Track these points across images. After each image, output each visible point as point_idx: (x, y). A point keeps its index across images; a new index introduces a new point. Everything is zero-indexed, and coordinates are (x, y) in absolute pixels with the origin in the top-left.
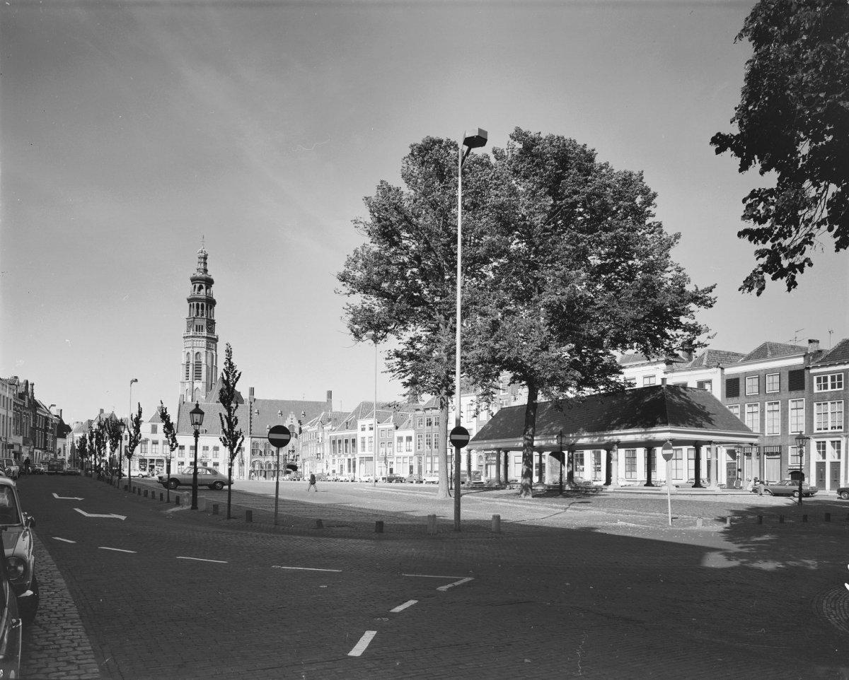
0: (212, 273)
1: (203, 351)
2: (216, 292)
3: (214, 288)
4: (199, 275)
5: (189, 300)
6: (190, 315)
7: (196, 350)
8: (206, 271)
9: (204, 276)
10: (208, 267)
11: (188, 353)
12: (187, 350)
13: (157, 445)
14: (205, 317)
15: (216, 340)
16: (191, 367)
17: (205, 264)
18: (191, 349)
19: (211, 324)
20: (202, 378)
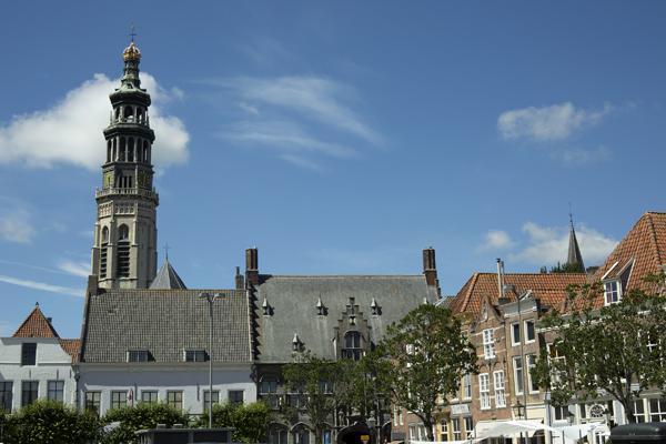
1: (132, 223)
4: (125, 89)
5: (108, 134)
6: (109, 160)
7: (120, 222)
8: (137, 83)
11: (106, 228)
12: (107, 222)
13: (27, 378)
18: (110, 219)
19: (147, 171)
20: (130, 272)
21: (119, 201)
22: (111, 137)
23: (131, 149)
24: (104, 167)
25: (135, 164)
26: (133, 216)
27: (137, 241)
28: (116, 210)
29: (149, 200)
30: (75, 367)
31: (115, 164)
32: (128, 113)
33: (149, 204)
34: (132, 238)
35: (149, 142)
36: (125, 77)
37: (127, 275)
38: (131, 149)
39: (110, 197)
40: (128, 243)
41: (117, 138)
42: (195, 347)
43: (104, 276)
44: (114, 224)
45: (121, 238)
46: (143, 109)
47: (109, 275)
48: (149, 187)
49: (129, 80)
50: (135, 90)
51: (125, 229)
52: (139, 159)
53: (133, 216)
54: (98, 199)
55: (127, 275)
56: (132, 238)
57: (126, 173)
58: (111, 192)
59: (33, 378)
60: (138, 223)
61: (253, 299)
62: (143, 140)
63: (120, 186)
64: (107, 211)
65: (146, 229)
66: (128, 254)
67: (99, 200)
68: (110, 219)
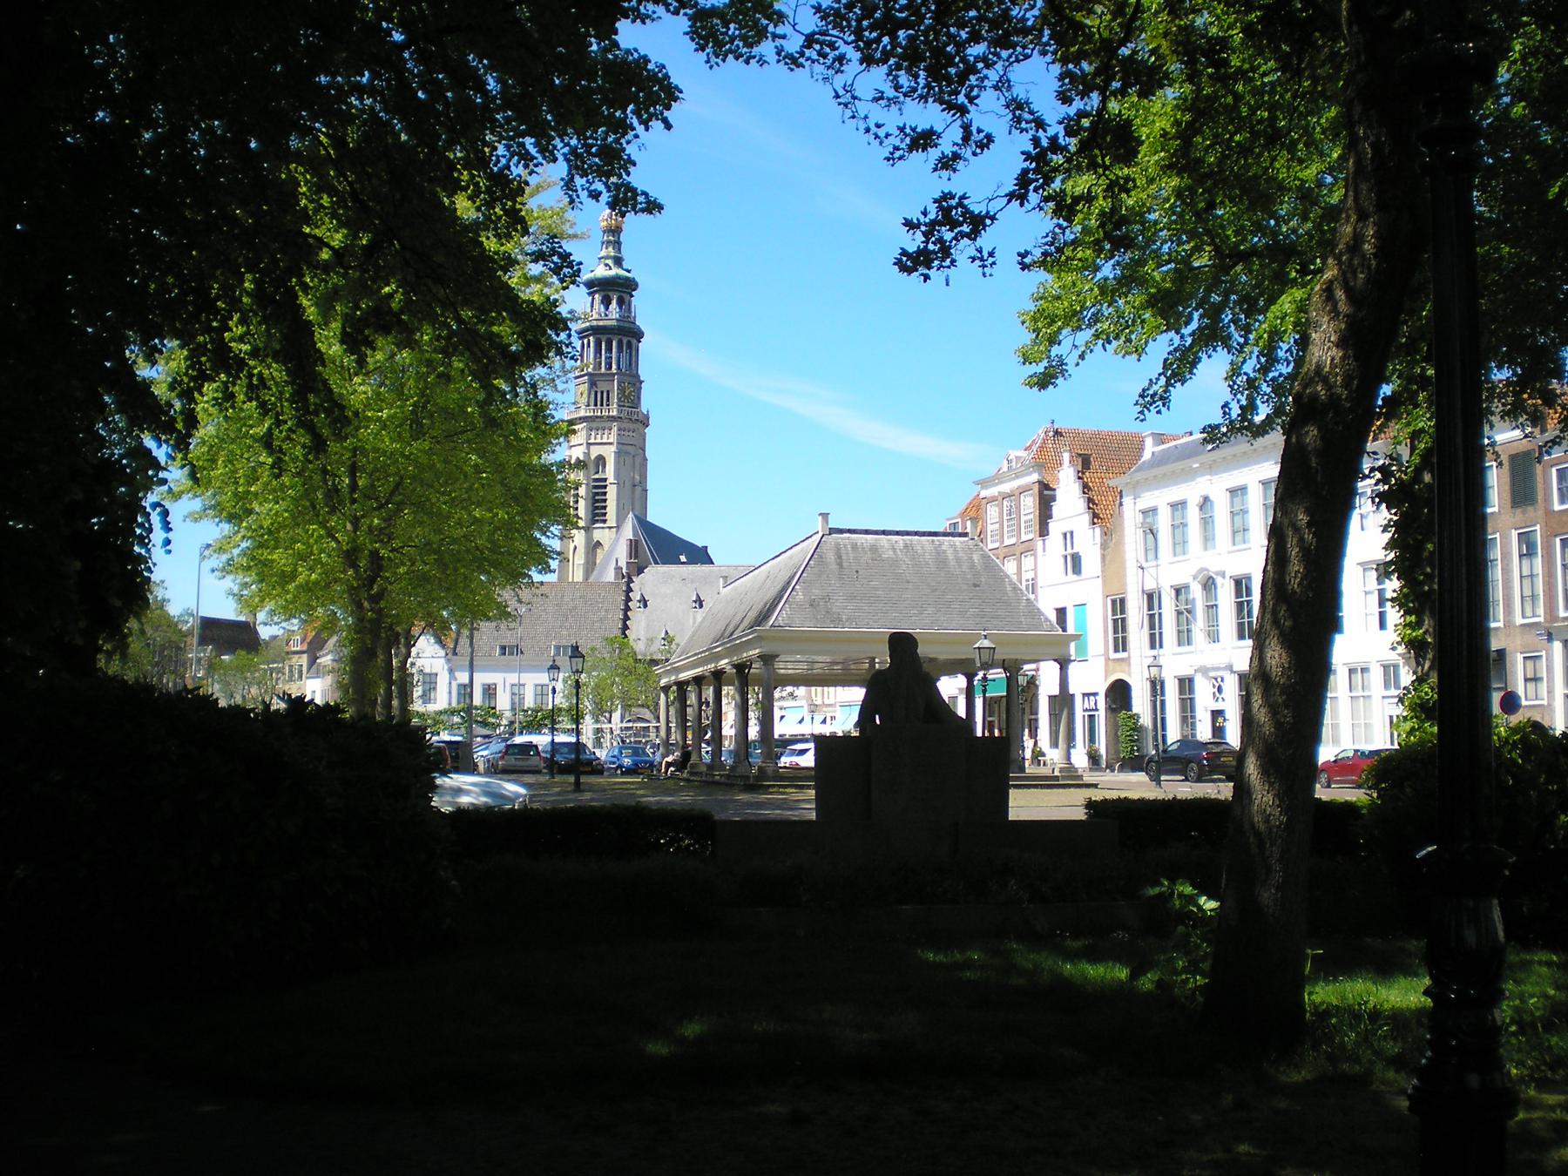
0: (635, 267)
1: (609, 453)
2: (643, 308)
3: (638, 300)
7: (595, 452)
8: (618, 261)
9: (615, 271)
14: (614, 369)
15: (645, 422)
17: (617, 244)
21: (594, 425)
23: (609, 349)
27: (617, 476)
28: (589, 437)
30: (448, 661)
32: (606, 302)
33: (639, 426)
34: (610, 472)
36: (603, 254)
38: (609, 349)
42: (564, 643)
46: (627, 297)
48: (636, 403)
49: (607, 257)
51: (601, 460)
56: (610, 472)
57: (602, 386)
58: (582, 413)
60: (618, 454)
61: (629, 590)
65: (629, 460)
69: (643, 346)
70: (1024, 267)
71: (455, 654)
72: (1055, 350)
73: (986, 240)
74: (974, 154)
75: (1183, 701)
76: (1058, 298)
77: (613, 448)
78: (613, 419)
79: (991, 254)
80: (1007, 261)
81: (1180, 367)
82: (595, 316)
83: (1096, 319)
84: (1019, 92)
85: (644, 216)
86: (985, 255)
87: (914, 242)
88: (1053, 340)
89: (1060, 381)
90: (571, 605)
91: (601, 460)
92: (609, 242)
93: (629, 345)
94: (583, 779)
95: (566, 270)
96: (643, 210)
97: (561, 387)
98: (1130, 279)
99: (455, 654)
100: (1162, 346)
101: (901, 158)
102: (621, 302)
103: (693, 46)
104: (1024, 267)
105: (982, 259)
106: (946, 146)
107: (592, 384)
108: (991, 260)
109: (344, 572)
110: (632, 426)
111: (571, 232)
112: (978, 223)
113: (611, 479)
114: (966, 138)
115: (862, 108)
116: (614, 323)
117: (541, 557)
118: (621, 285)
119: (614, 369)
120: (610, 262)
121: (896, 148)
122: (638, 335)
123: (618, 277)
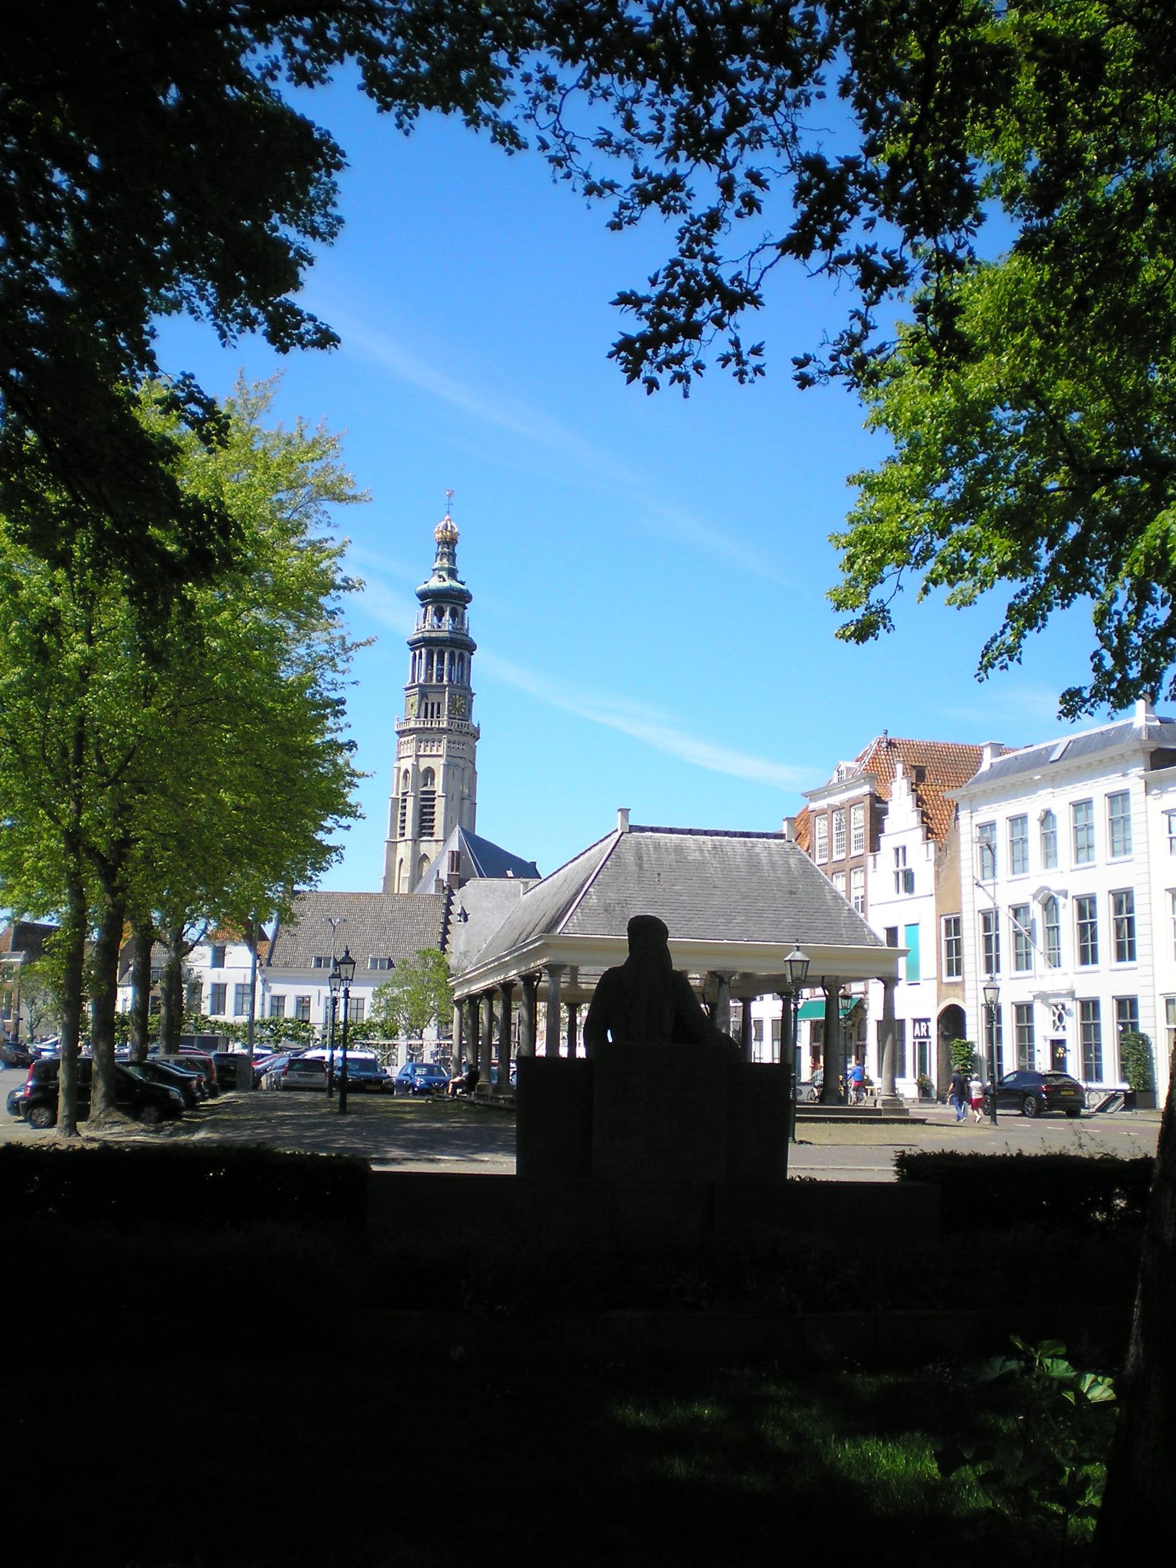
0: (470, 578)
1: (438, 765)
3: (471, 612)
4: (435, 583)
5: (414, 645)
7: (424, 764)
8: (452, 573)
9: (449, 583)
10: (459, 564)
11: (407, 771)
12: (407, 764)
13: (216, 981)
14: (445, 682)
16: (410, 804)
17: (452, 557)
20: (435, 830)
21: (424, 737)
22: (416, 648)
23: (441, 661)
24: (407, 689)
25: (445, 687)
26: (440, 756)
29: (464, 736)
31: (419, 686)
32: (439, 614)
33: (469, 739)
34: (438, 785)
35: (466, 654)
36: (437, 565)
37: (432, 835)
38: (441, 661)
39: (412, 731)
40: (434, 792)
41: (423, 650)
43: (403, 835)
44: (416, 767)
45: (426, 785)
46: (460, 609)
47: (408, 835)
50: (446, 584)
51: (430, 772)
52: (450, 680)
53: (440, 756)
54: (398, 733)
55: (432, 835)
56: (438, 785)
58: (412, 725)
59: (221, 981)
60: (447, 767)
61: (450, 903)
62: (457, 652)
63: (426, 717)
64: (409, 750)
65: (458, 773)
66: (433, 806)
67: (401, 733)
68: (411, 761)
69: (476, 659)
70: (805, 382)
71: (269, 964)
72: (879, 593)
73: (748, 324)
74: (739, 215)
75: (1083, 928)
76: (880, 521)
77: (442, 761)
78: (442, 731)
79: (756, 351)
80: (780, 370)
81: (1027, 615)
82: (428, 628)
83: (927, 553)
84: (807, 146)
85: (314, 352)
86: (745, 348)
87: (636, 326)
88: (874, 579)
89: (882, 632)
90: (390, 917)
91: (430, 772)
92: (443, 554)
93: (461, 657)
94: (352, 1098)
95: (211, 425)
96: (314, 344)
97: (341, 666)
98: (968, 505)
99: (269, 964)
100: (1007, 590)
101: (632, 220)
102: (454, 615)
103: (374, 104)
104: (805, 382)
105: (740, 362)
106: (699, 207)
107: (423, 696)
108: (754, 361)
109: (65, 856)
110: (462, 739)
111: (351, 493)
112: (738, 298)
113: (440, 792)
114: (727, 187)
115: (579, 162)
116: (447, 635)
117: (321, 855)
118: (454, 597)
119: (445, 682)
120: (444, 574)
121: (624, 206)
122: (471, 647)
123: (451, 589)
